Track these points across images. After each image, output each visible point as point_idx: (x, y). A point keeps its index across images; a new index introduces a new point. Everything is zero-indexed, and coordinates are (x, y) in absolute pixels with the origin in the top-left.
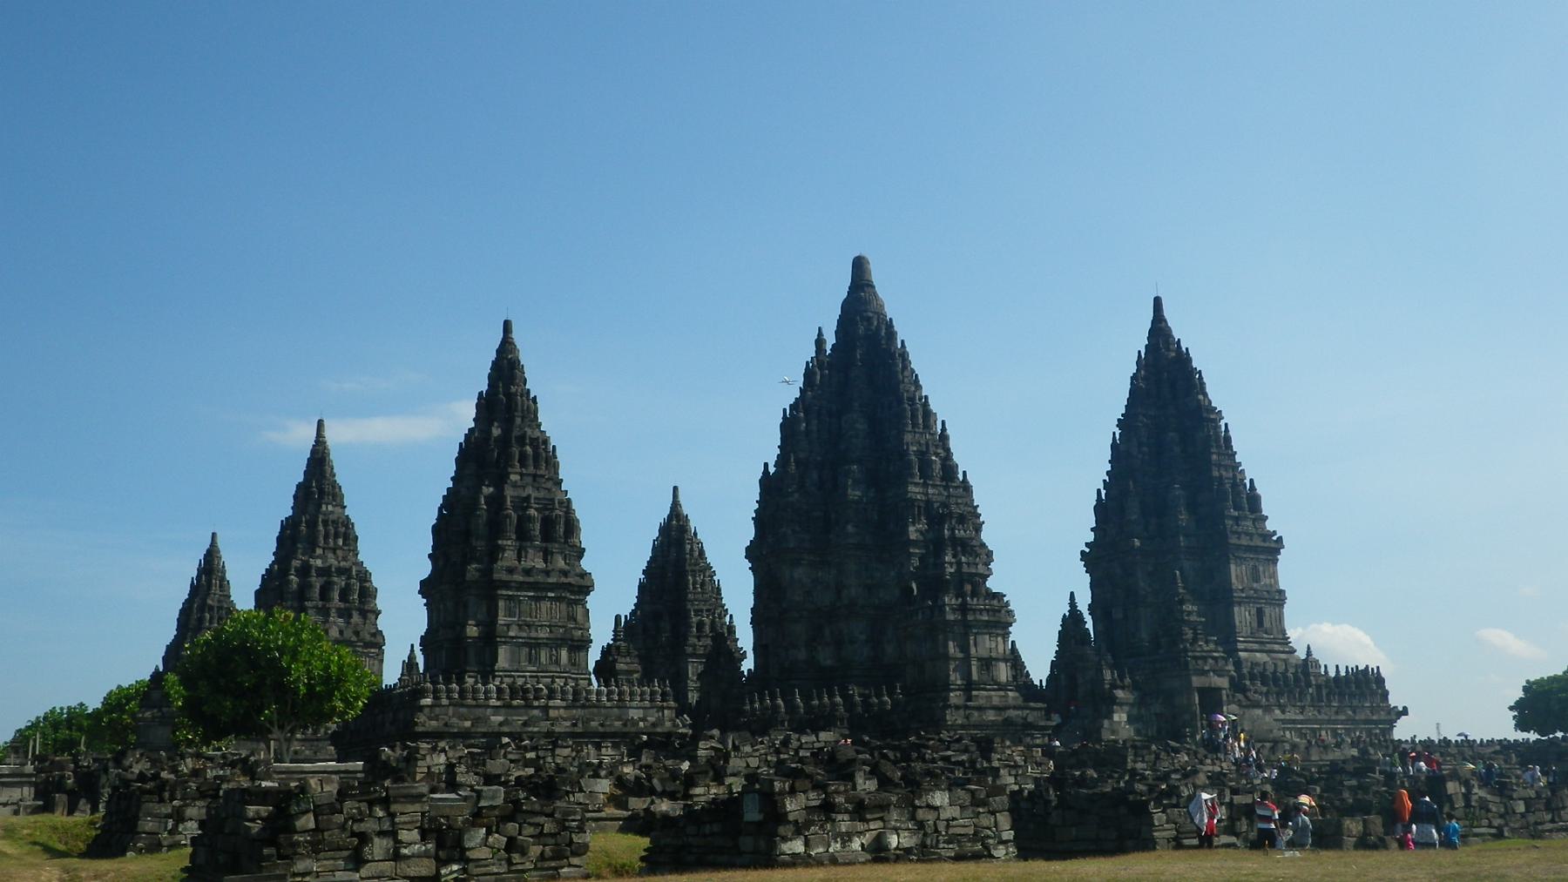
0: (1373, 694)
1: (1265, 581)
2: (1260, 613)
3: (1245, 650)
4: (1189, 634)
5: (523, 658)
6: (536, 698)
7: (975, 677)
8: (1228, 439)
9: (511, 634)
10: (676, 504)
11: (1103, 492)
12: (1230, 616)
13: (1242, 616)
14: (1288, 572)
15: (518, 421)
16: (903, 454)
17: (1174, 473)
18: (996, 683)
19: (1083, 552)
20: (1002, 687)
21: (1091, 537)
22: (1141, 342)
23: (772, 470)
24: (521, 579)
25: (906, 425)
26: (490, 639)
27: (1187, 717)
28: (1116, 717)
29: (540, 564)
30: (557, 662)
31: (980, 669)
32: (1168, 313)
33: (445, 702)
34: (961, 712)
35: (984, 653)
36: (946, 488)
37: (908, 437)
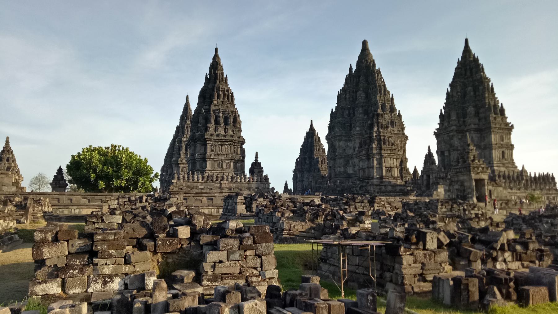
0: (550, 183)
1: (505, 141)
2: (503, 153)
3: (497, 166)
4: (472, 157)
5: (216, 166)
6: (217, 180)
7: (384, 174)
8: (492, 89)
9: (212, 157)
10: (312, 126)
11: (443, 111)
12: (491, 154)
13: (496, 154)
14: (515, 138)
15: (218, 82)
16: (376, 104)
17: (471, 103)
18: (392, 176)
19: (434, 132)
20: (395, 178)
21: (438, 127)
22: (459, 55)
23: (334, 111)
24: (215, 138)
25: (377, 94)
26: (204, 159)
27: (469, 191)
28: (439, 190)
29: (223, 133)
30: (229, 168)
31: (387, 171)
32: (470, 44)
33: (182, 180)
34: (378, 187)
35: (388, 165)
36: (391, 114)
37: (378, 98)
